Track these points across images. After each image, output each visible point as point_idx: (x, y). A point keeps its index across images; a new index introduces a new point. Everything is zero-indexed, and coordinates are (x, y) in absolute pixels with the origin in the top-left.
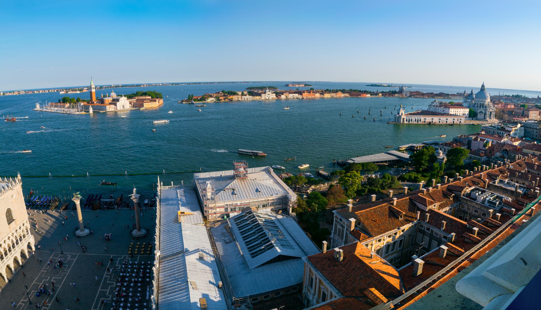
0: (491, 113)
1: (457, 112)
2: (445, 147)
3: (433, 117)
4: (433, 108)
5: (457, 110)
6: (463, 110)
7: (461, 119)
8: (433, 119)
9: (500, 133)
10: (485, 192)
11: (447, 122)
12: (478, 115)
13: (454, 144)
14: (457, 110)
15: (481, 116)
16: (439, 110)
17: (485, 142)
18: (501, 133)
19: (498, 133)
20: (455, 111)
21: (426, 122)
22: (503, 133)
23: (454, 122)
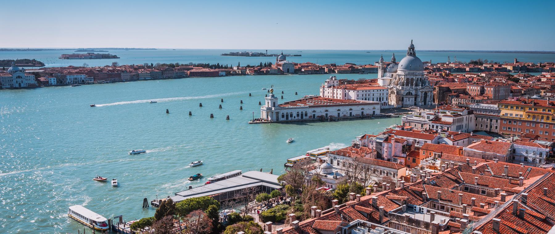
0: (426, 94)
1: (367, 95)
2: (337, 157)
3: (327, 106)
4: (328, 91)
5: (369, 93)
6: (379, 92)
7: (374, 108)
8: (327, 111)
9: (433, 126)
10: (374, 227)
11: (351, 113)
12: (405, 99)
13: (352, 150)
14: (369, 93)
15: (409, 100)
16: (339, 94)
17: (405, 143)
18: (435, 126)
19: (430, 128)
20: (364, 95)
21: (316, 116)
22: (437, 127)
23: (362, 112)
